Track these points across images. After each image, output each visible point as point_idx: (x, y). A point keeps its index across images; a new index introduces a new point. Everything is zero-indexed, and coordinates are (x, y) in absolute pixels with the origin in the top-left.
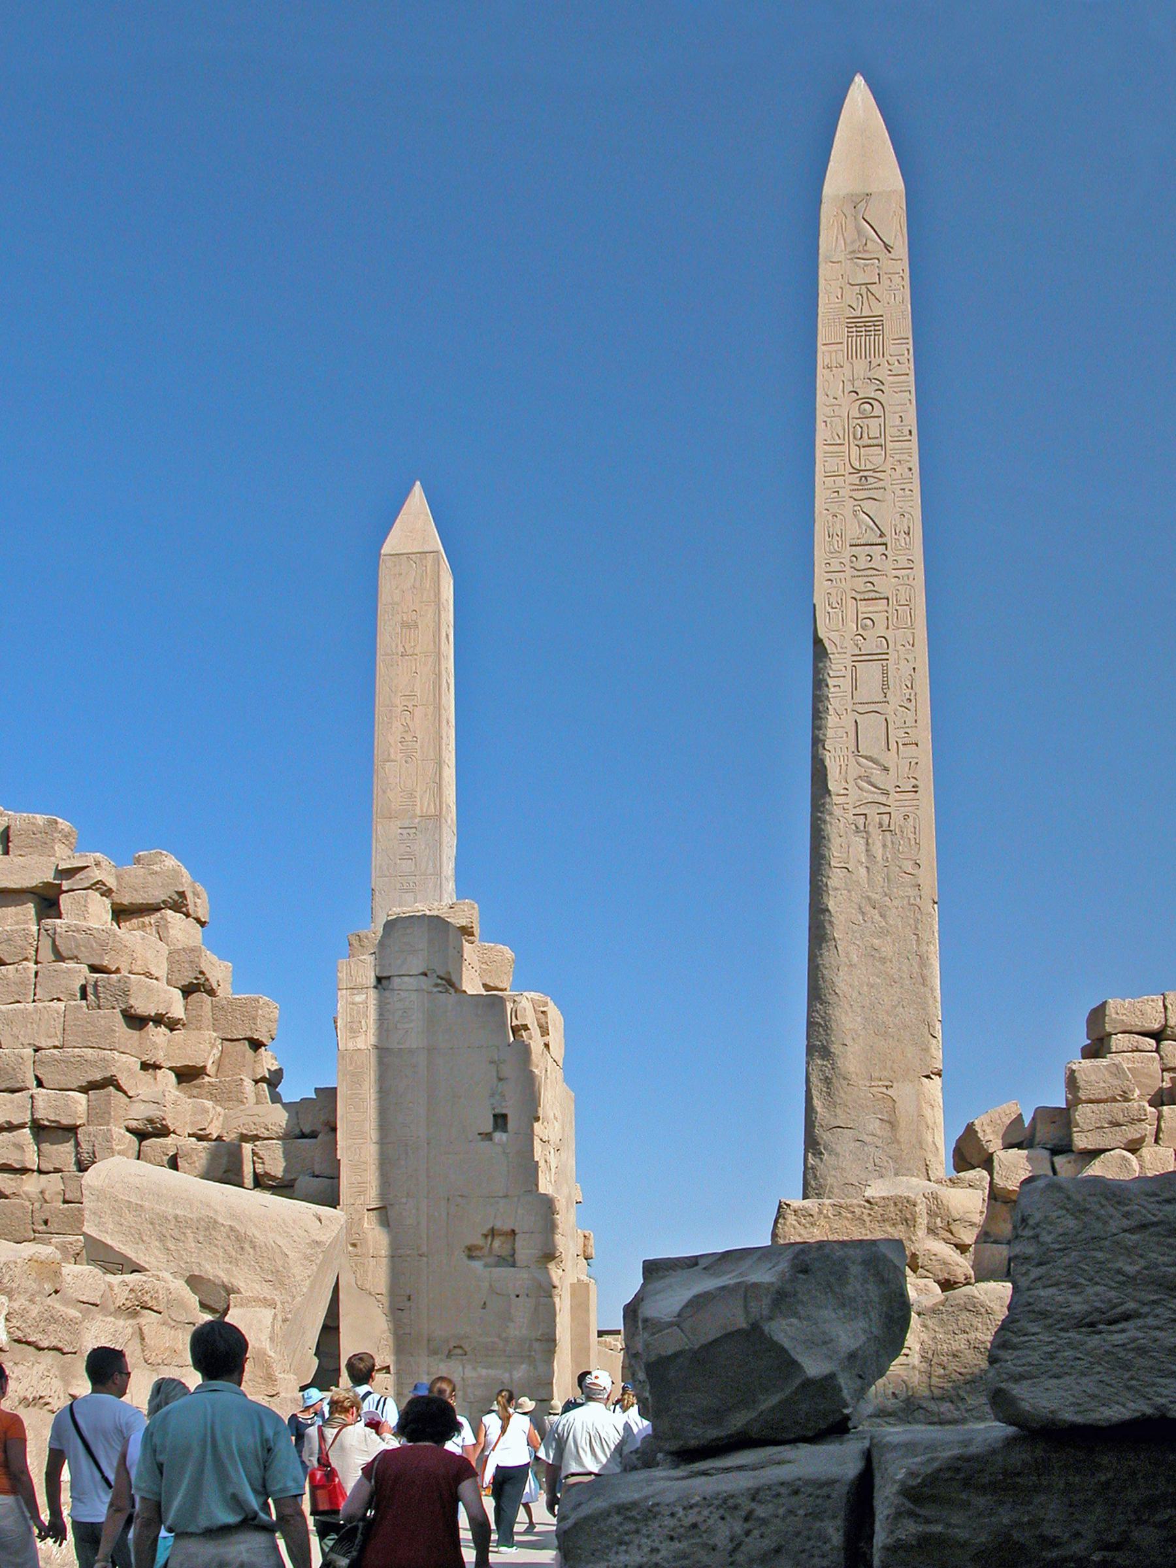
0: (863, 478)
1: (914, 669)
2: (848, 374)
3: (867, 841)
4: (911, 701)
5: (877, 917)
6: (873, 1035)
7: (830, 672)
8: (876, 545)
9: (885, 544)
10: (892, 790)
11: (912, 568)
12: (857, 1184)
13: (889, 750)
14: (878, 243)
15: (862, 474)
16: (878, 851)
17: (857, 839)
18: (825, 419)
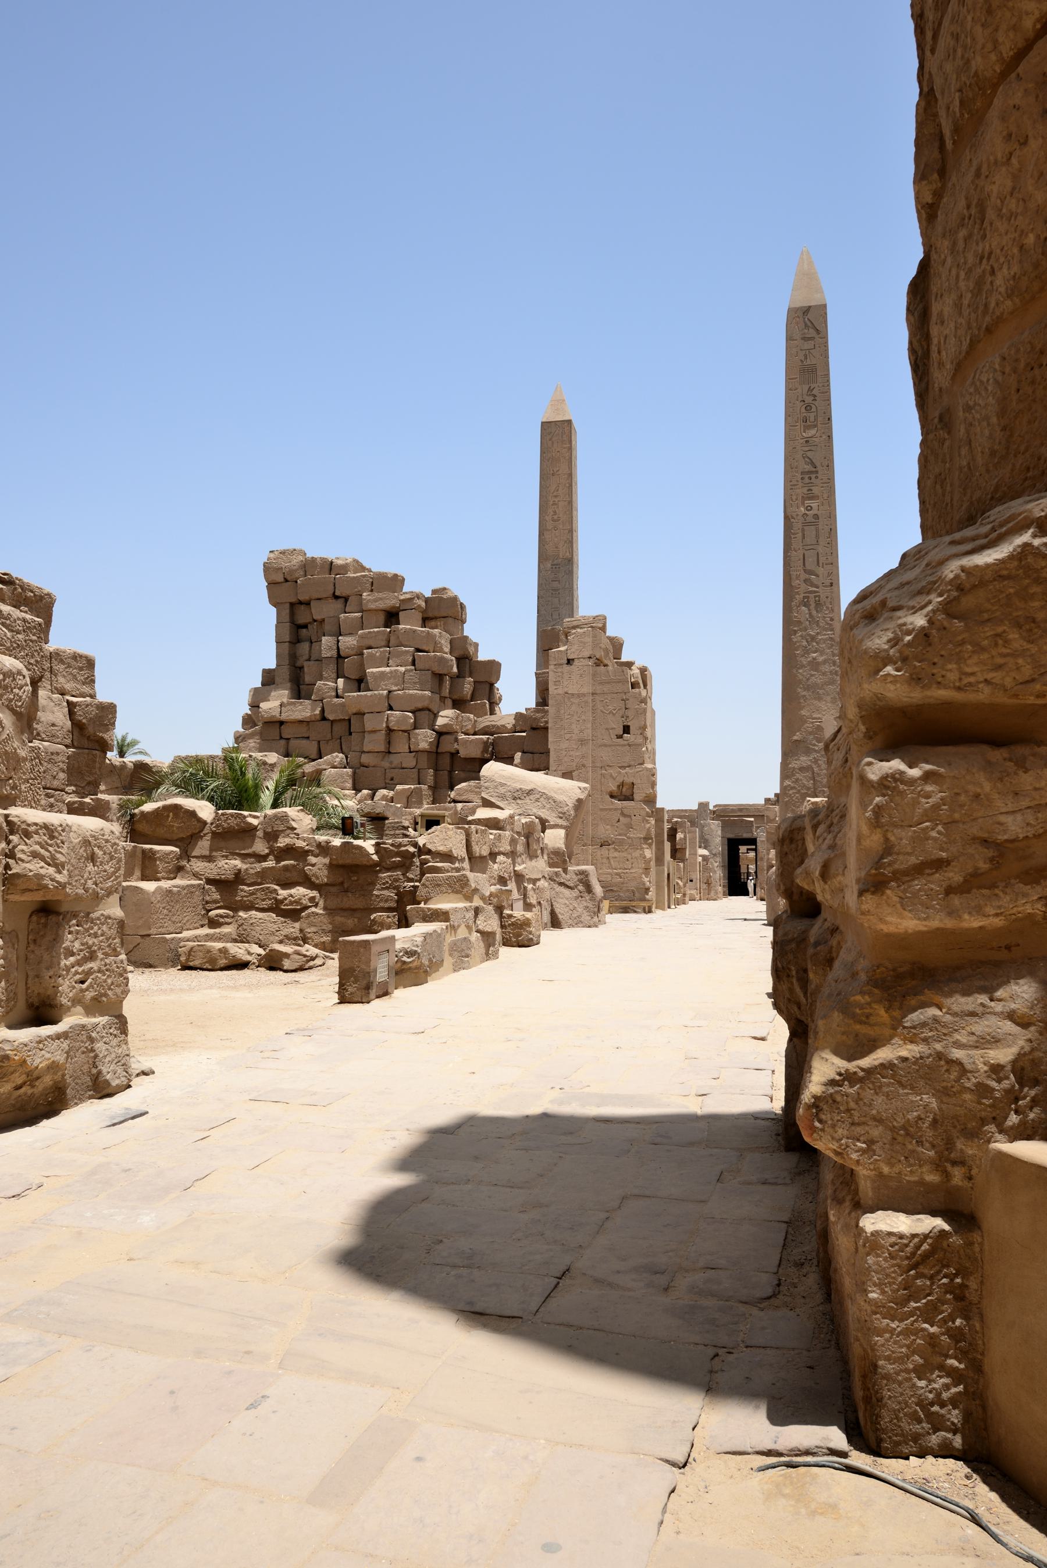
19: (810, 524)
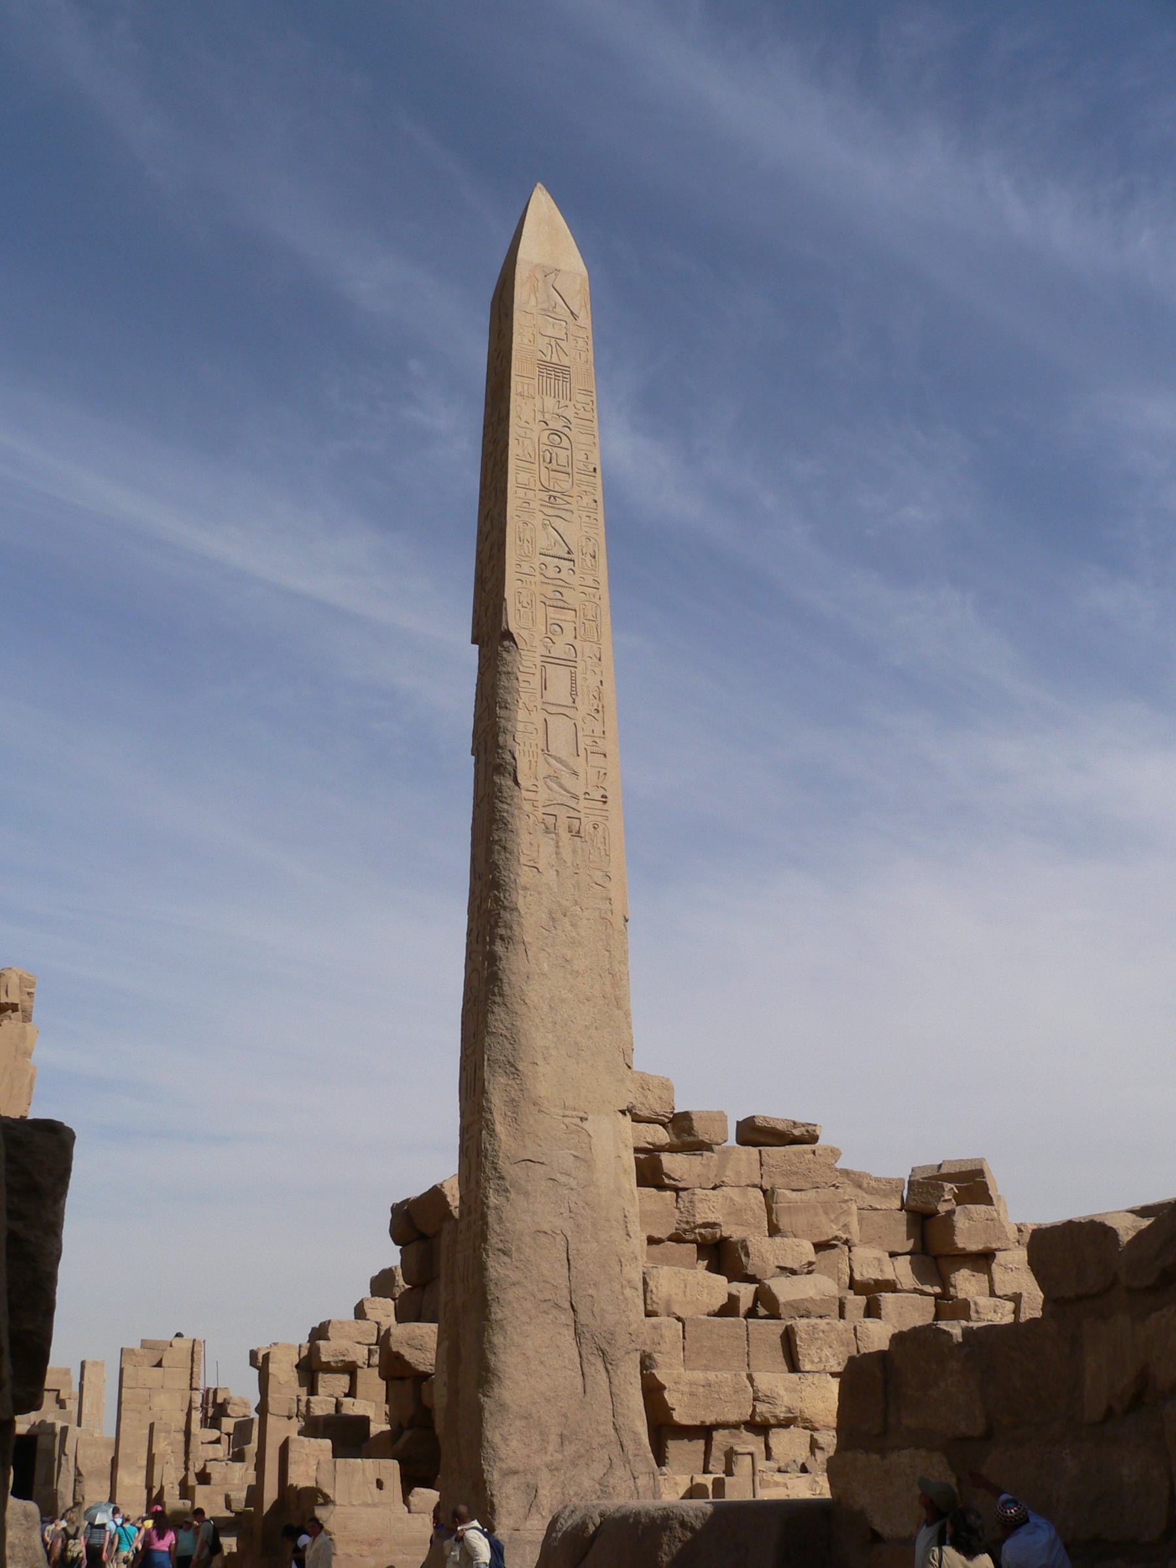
0: (552, 498)
1: (601, 682)
2: (539, 406)
3: (557, 842)
4: (598, 712)
5: (568, 926)
6: (566, 1056)
7: (520, 667)
8: (564, 559)
9: (574, 561)
10: (582, 797)
11: (598, 589)
12: (550, 1232)
13: (578, 755)
14: (566, 310)
15: (551, 493)
16: (566, 853)
17: (546, 839)
18: (519, 438)
19: (558, 662)
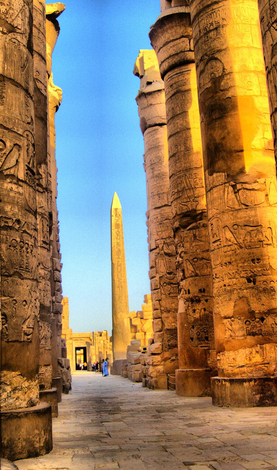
16: (121, 289)
